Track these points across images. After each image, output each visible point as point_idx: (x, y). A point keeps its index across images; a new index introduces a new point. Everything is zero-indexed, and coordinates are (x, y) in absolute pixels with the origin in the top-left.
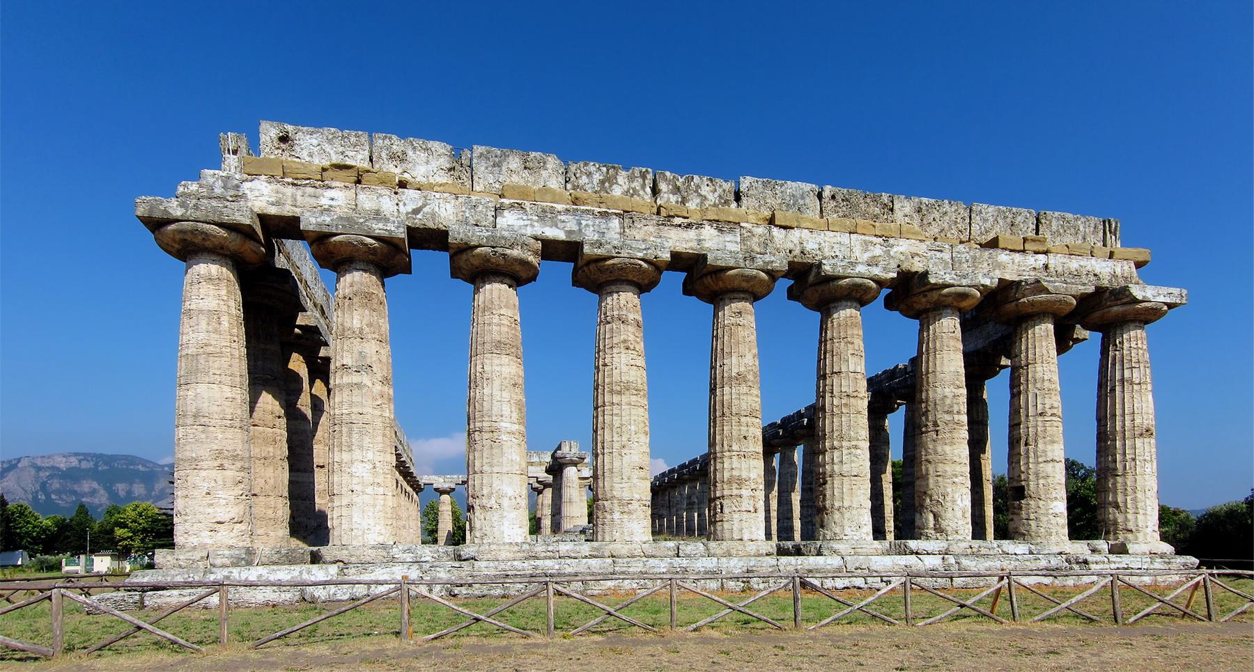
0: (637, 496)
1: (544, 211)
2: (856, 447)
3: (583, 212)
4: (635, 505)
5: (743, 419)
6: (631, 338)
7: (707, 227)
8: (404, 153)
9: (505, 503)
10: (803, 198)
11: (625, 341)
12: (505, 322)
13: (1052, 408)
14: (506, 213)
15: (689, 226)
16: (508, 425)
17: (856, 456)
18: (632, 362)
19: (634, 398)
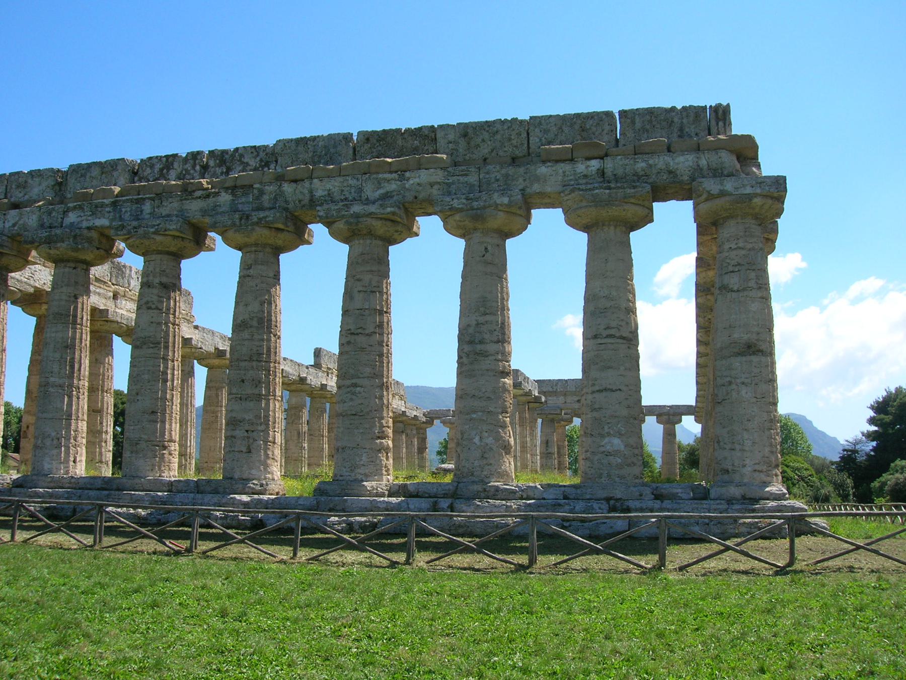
0: (146, 437)
1: (96, 207)
2: (355, 385)
3: (124, 201)
4: (143, 445)
5: (243, 364)
6: (155, 298)
7: (223, 194)
8: (26, 182)
9: (48, 442)
10: (335, 147)
11: (147, 303)
12: (64, 297)
13: (608, 328)
14: (70, 214)
15: (208, 196)
16: (57, 380)
17: (354, 394)
18: (153, 320)
19: (151, 351)
